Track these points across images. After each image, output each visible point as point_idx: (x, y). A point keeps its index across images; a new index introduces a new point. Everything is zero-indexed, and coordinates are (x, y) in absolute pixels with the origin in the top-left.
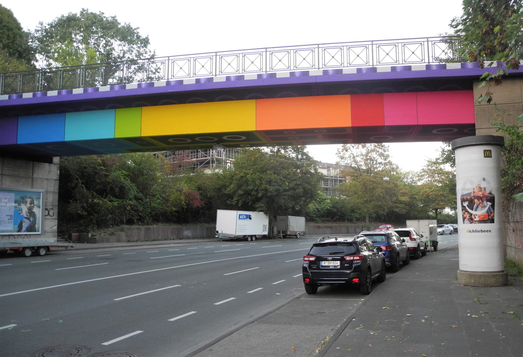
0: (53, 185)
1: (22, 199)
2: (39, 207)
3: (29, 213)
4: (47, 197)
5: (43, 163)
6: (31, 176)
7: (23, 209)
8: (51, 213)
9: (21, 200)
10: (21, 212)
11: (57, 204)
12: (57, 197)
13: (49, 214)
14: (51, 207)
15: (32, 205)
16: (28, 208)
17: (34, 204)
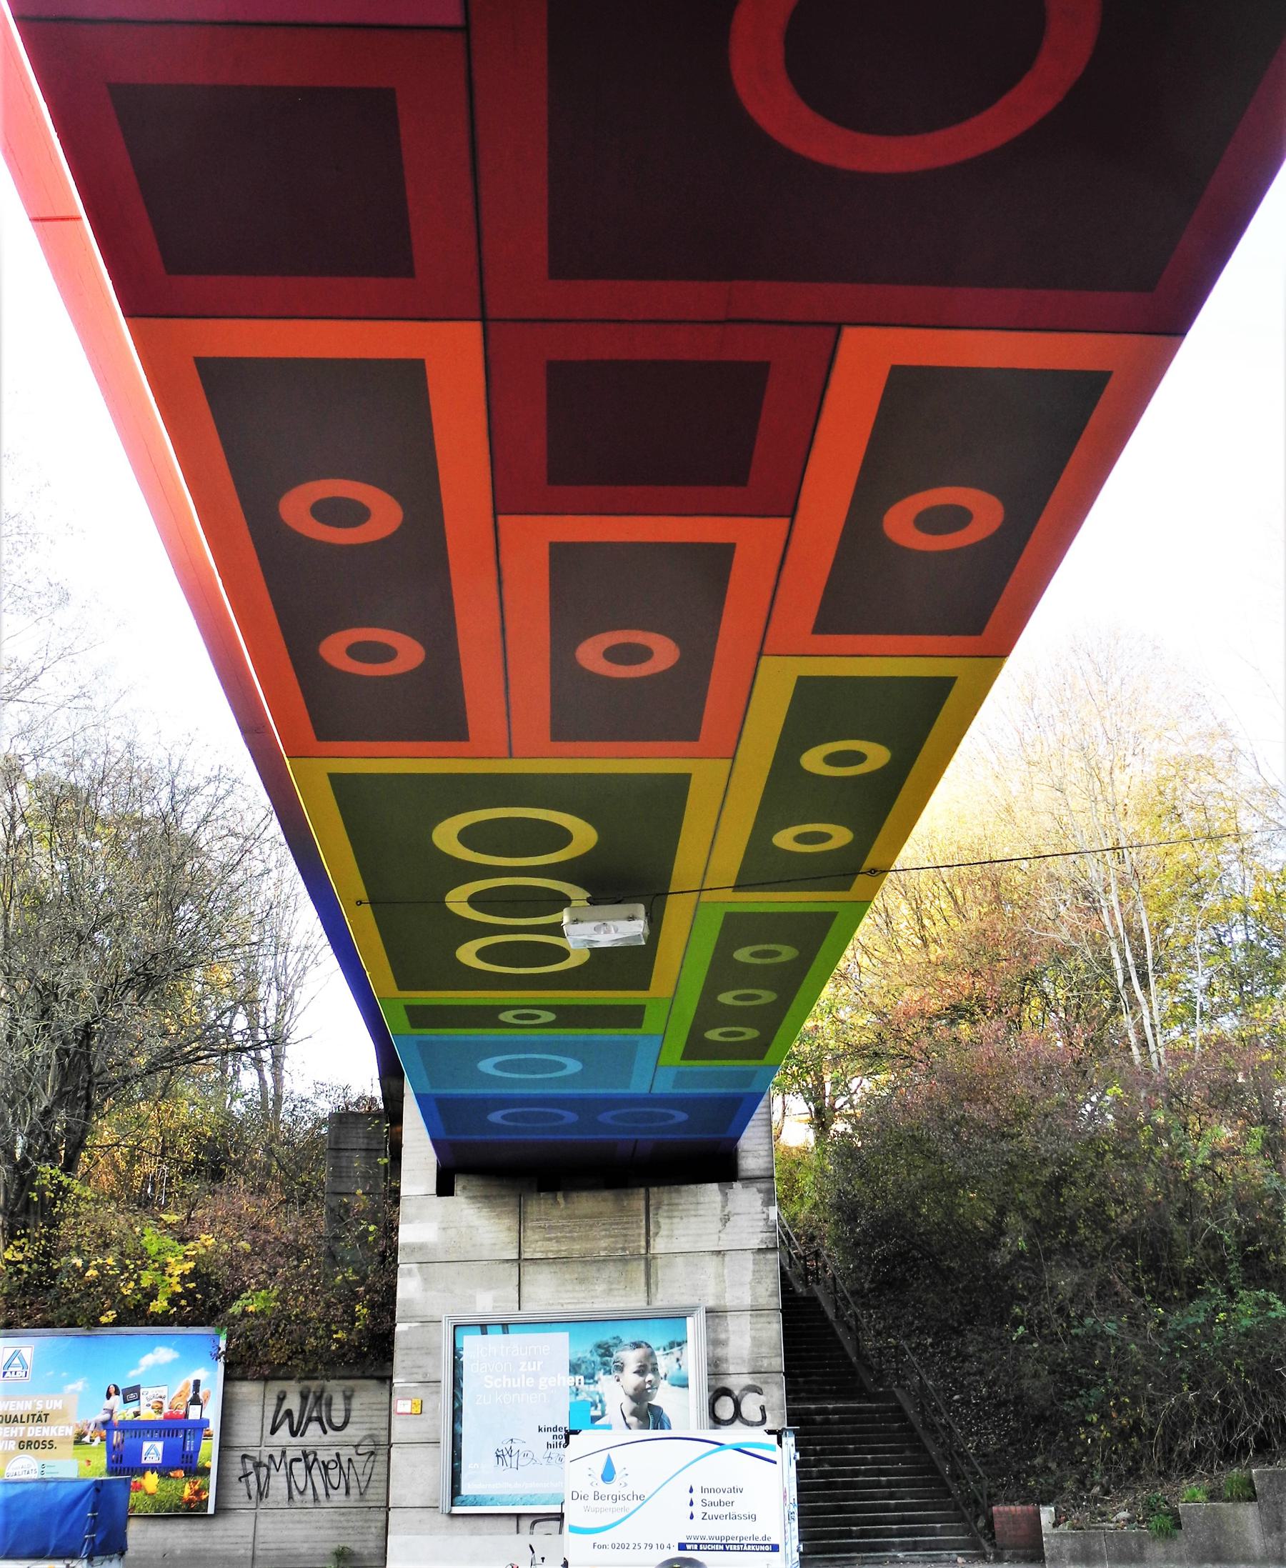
0: (749, 1276)
1: (602, 1356)
2: (684, 1385)
3: (634, 1413)
4: (723, 1336)
5: (693, 1187)
6: (643, 1251)
7: (605, 1399)
8: (751, 1407)
9: (598, 1359)
10: (598, 1413)
11: (779, 1363)
12: (774, 1329)
13: (737, 1414)
14: (747, 1380)
15: (650, 1377)
16: (631, 1391)
17: (655, 1371)
